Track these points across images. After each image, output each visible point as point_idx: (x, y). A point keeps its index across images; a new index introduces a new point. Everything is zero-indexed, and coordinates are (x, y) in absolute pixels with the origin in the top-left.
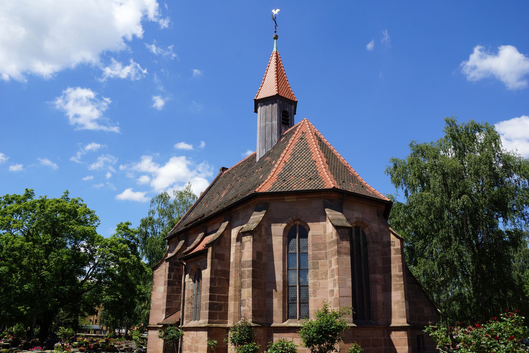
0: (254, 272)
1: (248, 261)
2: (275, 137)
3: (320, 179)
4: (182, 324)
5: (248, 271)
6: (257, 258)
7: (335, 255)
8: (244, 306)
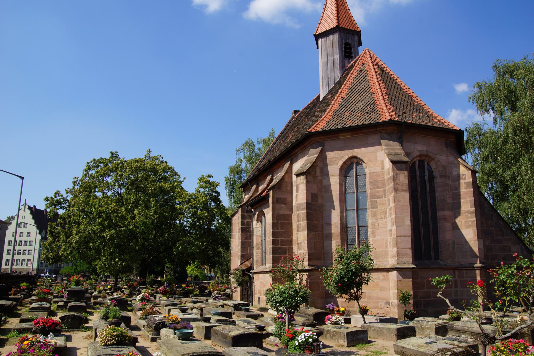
0: (308, 214)
1: (302, 204)
2: (338, 74)
5: (303, 214)
6: (312, 200)
7: (391, 193)
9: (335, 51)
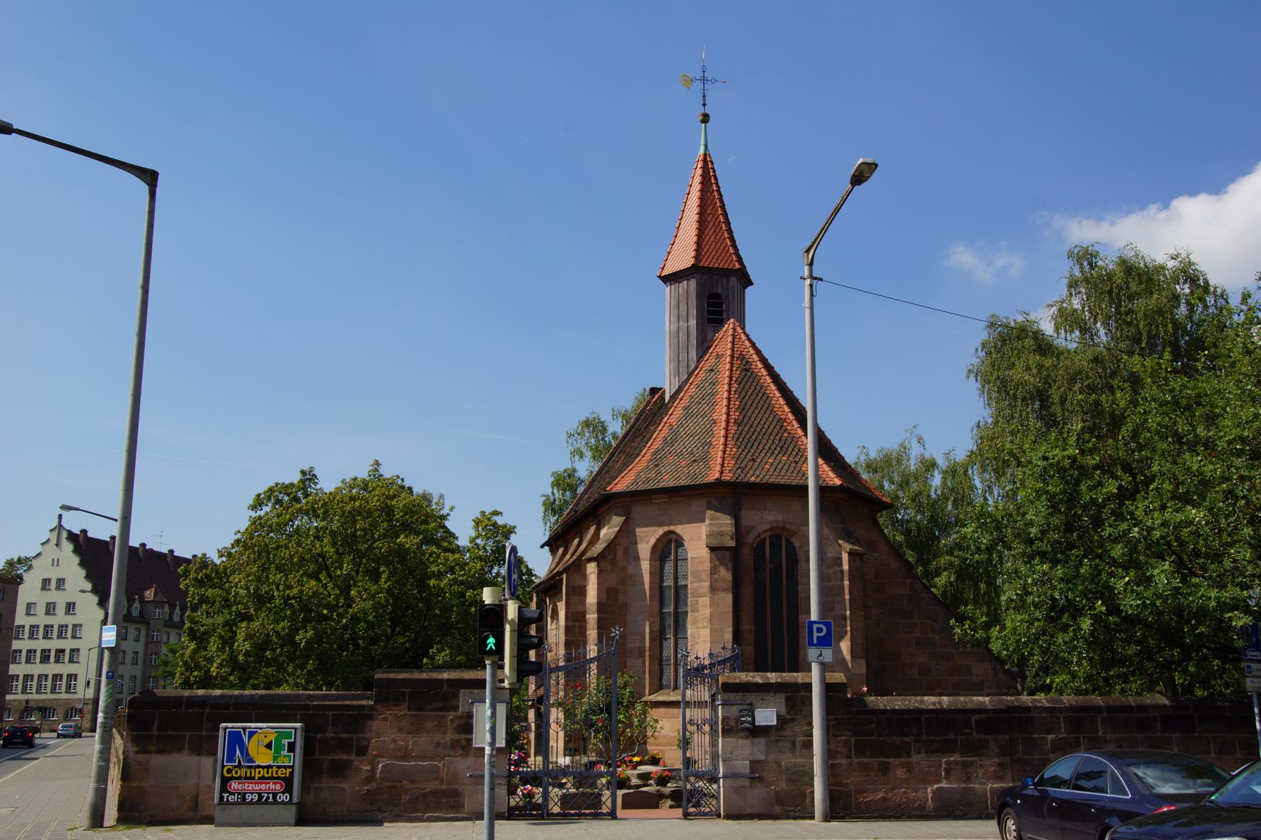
2: (693, 354)
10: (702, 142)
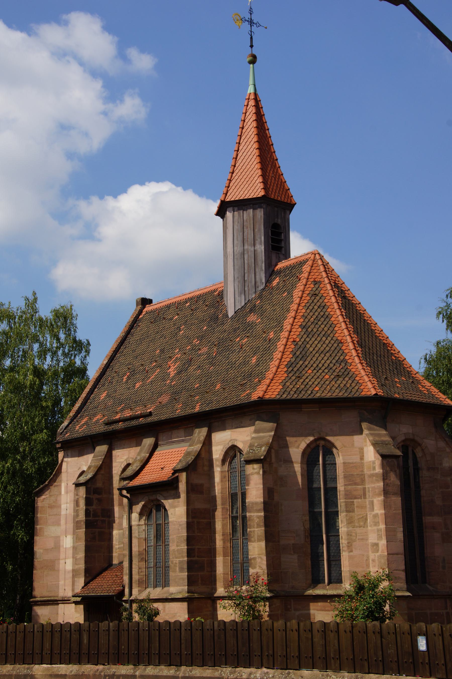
1: (256, 503)
2: (262, 276)
3: (353, 377)
4: (131, 594)
5: (258, 517)
7: (379, 495)
8: (254, 568)
9: (257, 237)
10: (251, 82)
